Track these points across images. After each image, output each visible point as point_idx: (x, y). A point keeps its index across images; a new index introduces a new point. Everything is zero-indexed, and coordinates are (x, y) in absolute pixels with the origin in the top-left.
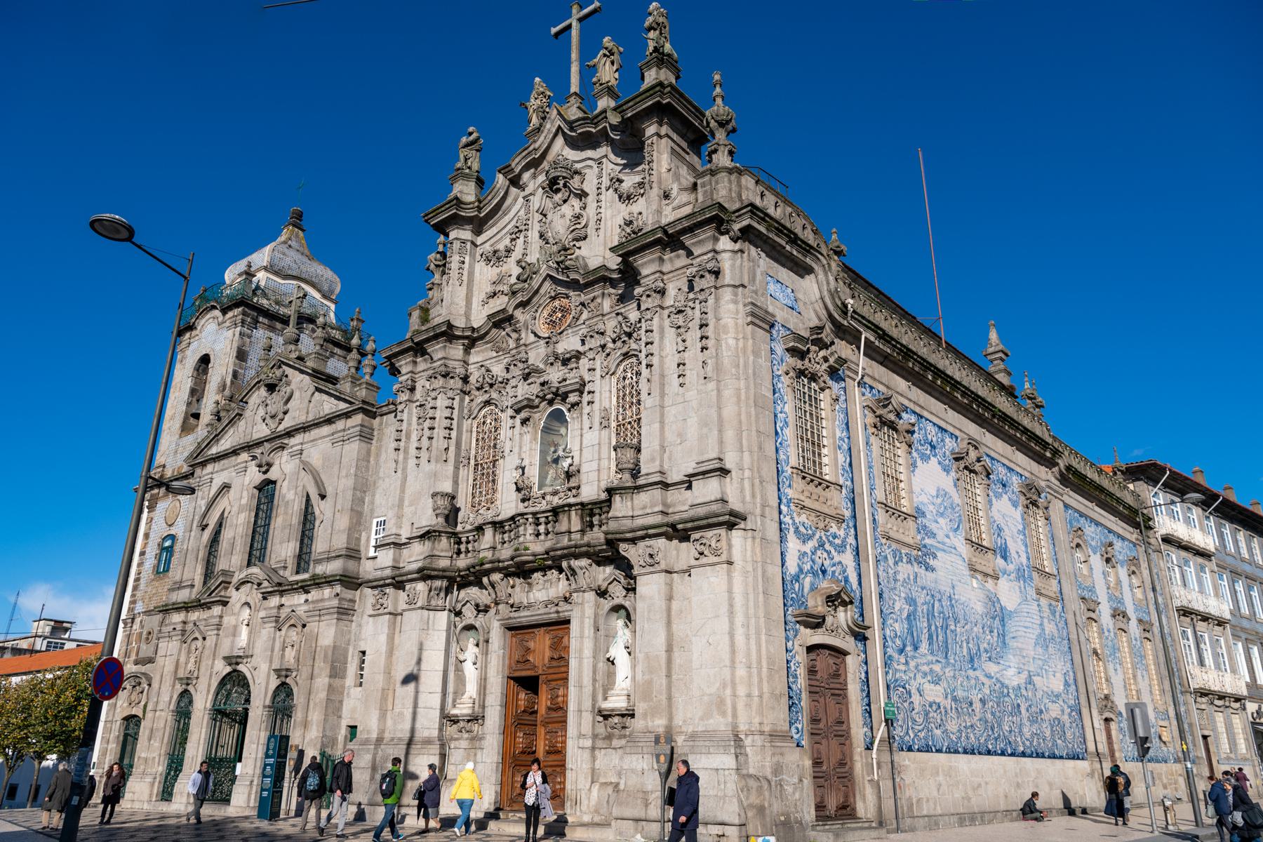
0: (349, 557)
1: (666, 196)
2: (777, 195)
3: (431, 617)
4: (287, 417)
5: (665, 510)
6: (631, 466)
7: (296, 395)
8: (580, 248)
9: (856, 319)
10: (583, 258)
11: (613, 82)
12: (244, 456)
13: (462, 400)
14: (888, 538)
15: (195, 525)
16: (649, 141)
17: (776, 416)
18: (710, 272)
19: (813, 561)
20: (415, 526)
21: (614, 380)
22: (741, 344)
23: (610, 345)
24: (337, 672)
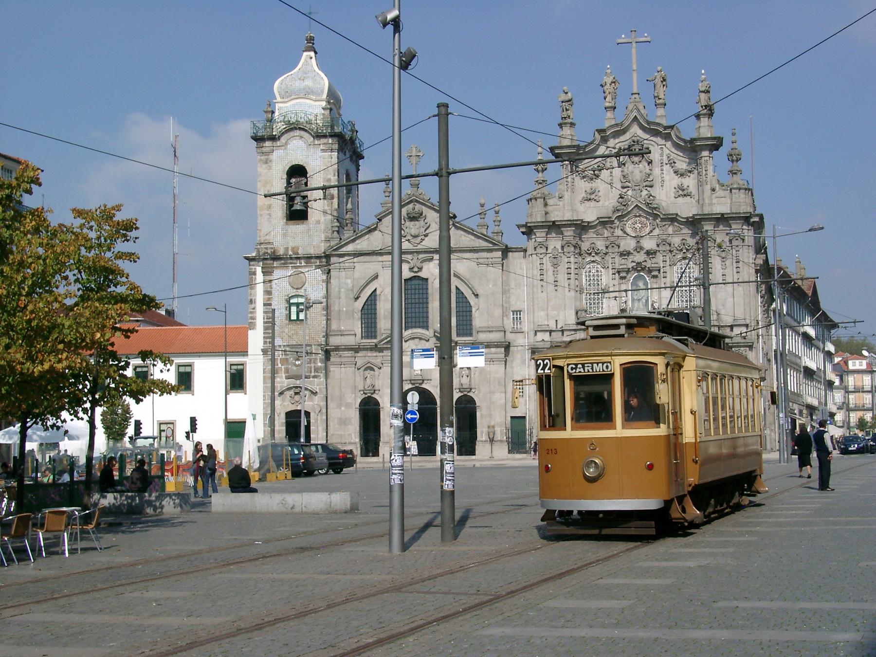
1: (713, 190)
4: (426, 239)
15: (343, 295)
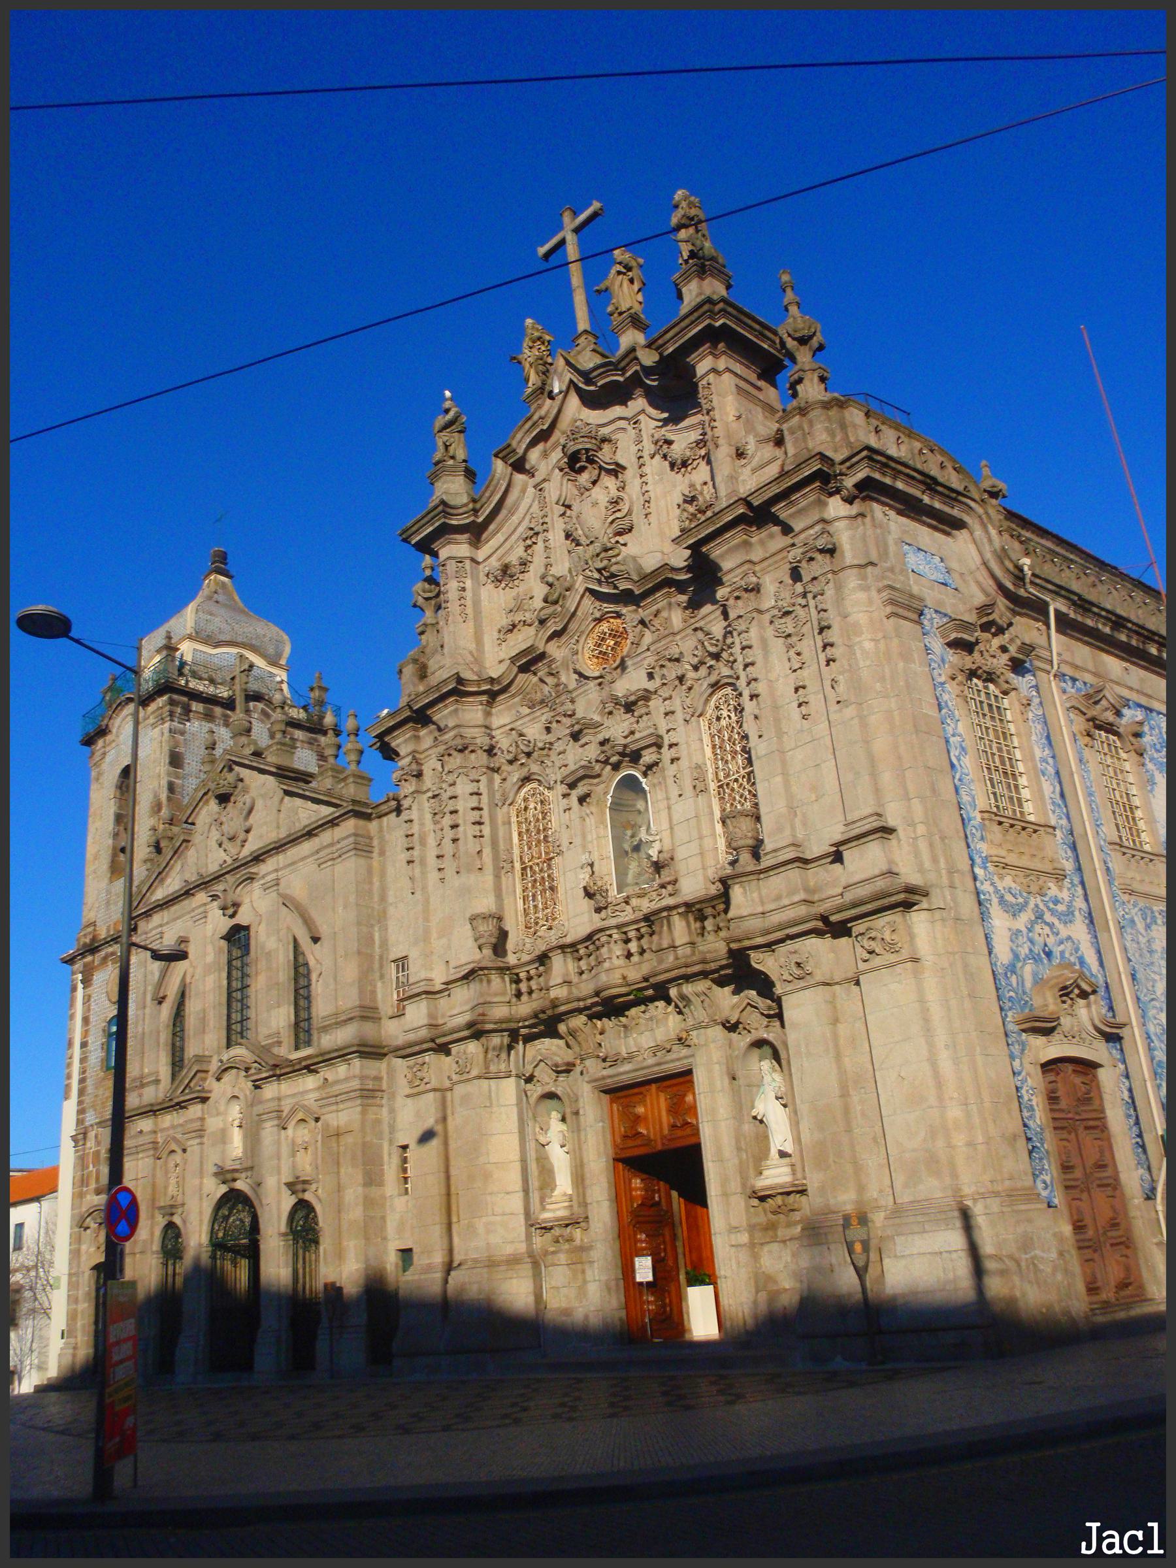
0: (364, 1018)
1: (740, 454)
2: (897, 427)
3: (493, 1088)
4: (251, 836)
5: (810, 898)
6: (750, 842)
7: (259, 804)
8: (625, 545)
9: (1037, 585)
10: (634, 558)
11: (637, 308)
12: (201, 897)
13: (491, 781)
14: (1132, 893)
16: (704, 382)
17: (947, 741)
18: (821, 551)
19: (1032, 941)
20: (452, 964)
21: (704, 723)
22: (882, 645)
23: (691, 674)
24: (372, 1179)
